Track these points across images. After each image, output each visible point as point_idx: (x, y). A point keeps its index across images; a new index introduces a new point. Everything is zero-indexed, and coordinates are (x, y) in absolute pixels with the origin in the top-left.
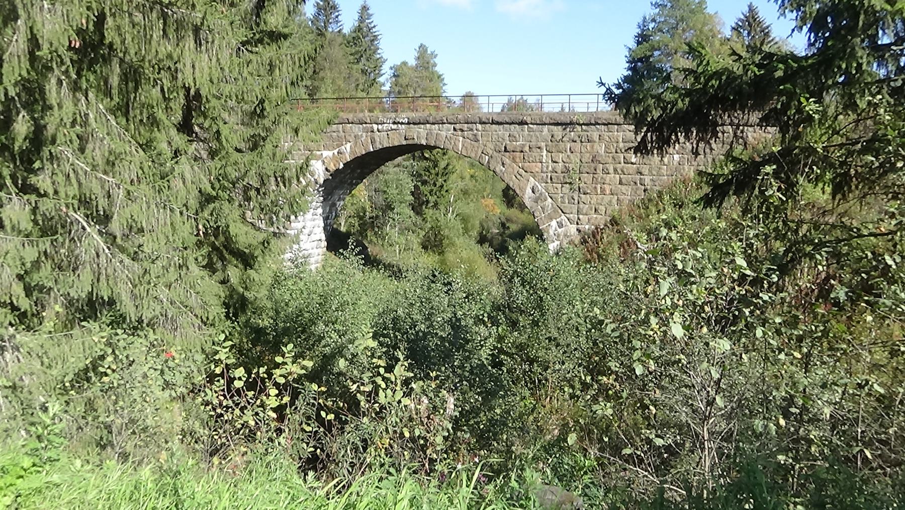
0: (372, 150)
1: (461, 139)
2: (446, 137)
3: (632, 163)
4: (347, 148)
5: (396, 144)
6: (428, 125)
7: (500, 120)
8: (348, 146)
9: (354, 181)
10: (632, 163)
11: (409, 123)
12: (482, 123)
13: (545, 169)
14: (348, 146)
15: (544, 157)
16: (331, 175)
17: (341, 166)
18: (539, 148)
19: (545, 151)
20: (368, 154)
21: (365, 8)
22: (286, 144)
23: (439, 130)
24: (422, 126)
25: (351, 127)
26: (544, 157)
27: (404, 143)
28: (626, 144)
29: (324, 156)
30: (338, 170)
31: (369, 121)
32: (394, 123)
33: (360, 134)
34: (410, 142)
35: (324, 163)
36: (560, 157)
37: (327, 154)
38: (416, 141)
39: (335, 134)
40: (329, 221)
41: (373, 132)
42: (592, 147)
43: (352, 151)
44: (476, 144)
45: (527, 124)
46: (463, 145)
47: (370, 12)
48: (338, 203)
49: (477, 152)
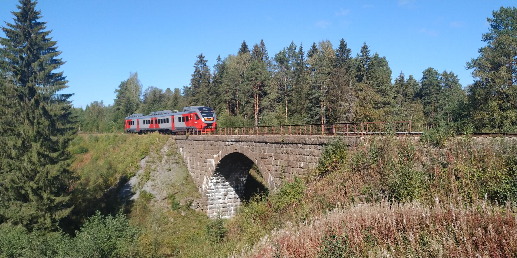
0: (226, 155)
3: (301, 168)
4: (220, 153)
5: (233, 152)
6: (240, 143)
7: (259, 141)
9: (243, 168)
10: (301, 168)
11: (235, 142)
12: (255, 142)
15: (273, 162)
16: (217, 166)
17: (219, 163)
18: (271, 157)
19: (274, 159)
20: (226, 156)
21: (365, 48)
26: (273, 162)
27: (235, 151)
28: (300, 156)
29: (215, 157)
30: (218, 164)
31: (224, 140)
32: (232, 141)
35: (215, 161)
36: (279, 161)
37: (215, 156)
39: (217, 146)
40: (239, 188)
41: (226, 145)
42: (288, 157)
43: (221, 155)
45: (268, 143)
47: (368, 49)
48: (242, 179)
49: (254, 157)
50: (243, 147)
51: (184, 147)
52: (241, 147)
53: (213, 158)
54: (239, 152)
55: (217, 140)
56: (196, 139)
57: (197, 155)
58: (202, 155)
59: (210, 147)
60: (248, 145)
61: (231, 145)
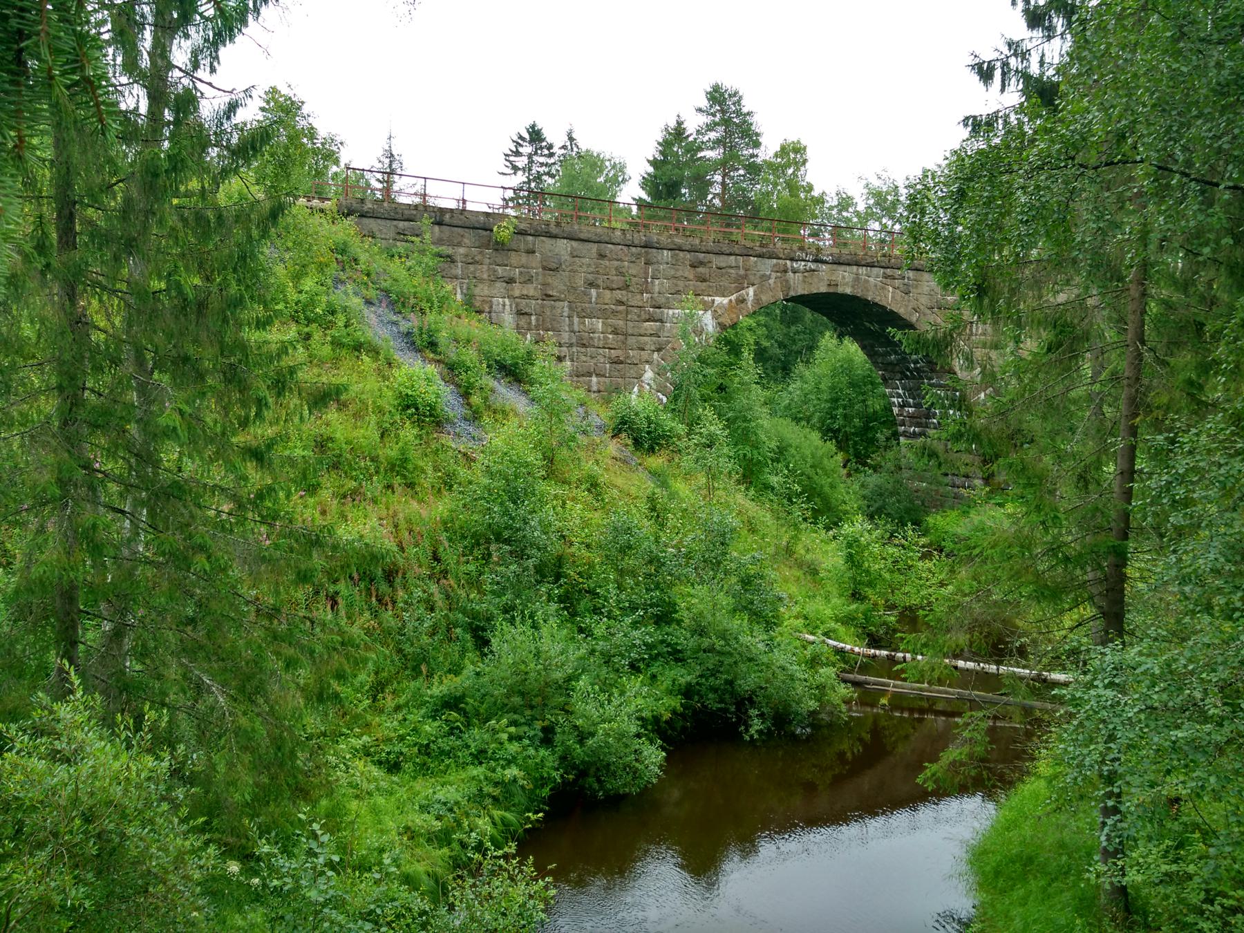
1: (891, 289)
2: (876, 286)
6: (855, 268)
8: (751, 291)
13: (974, 330)
14: (751, 291)
22: (657, 282)
23: (867, 275)
24: (848, 268)
25: (755, 262)
27: (823, 289)
29: (716, 303)
32: (816, 261)
33: (768, 273)
34: (832, 290)
37: (718, 300)
38: (840, 290)
44: (906, 297)
46: (892, 297)
50: (867, 281)
51: (458, 258)
52: (857, 278)
53: (707, 307)
54: (848, 291)
55: (737, 252)
56: (582, 236)
57: (590, 294)
58: (619, 295)
59: (689, 273)
60: (886, 277)
61: (814, 271)
